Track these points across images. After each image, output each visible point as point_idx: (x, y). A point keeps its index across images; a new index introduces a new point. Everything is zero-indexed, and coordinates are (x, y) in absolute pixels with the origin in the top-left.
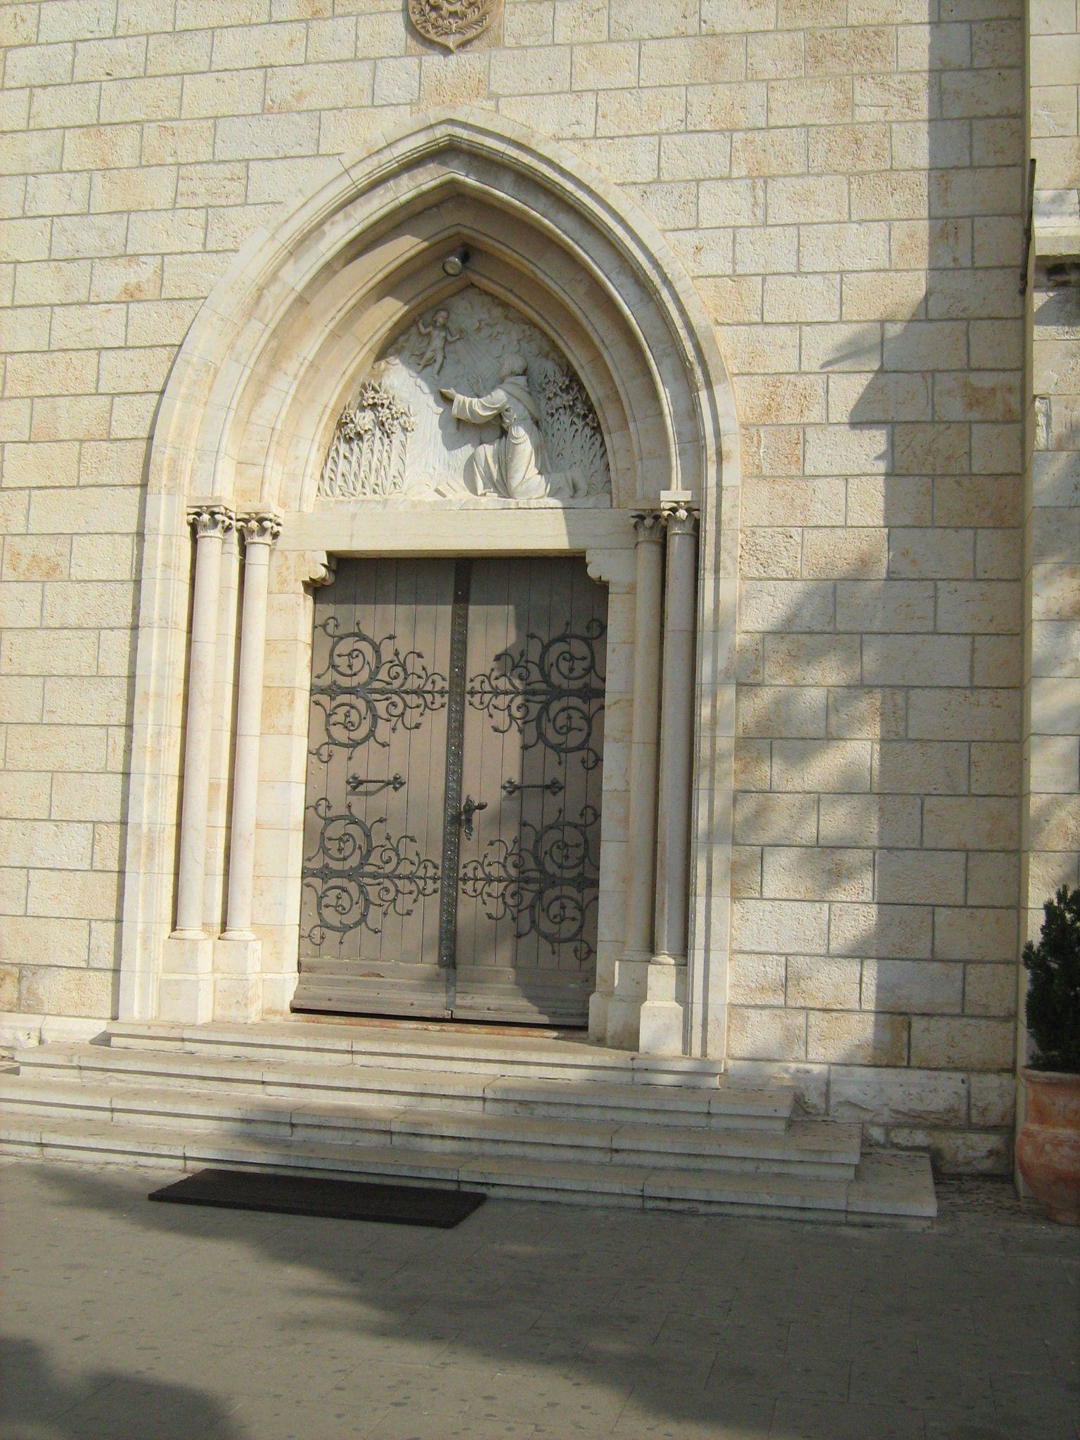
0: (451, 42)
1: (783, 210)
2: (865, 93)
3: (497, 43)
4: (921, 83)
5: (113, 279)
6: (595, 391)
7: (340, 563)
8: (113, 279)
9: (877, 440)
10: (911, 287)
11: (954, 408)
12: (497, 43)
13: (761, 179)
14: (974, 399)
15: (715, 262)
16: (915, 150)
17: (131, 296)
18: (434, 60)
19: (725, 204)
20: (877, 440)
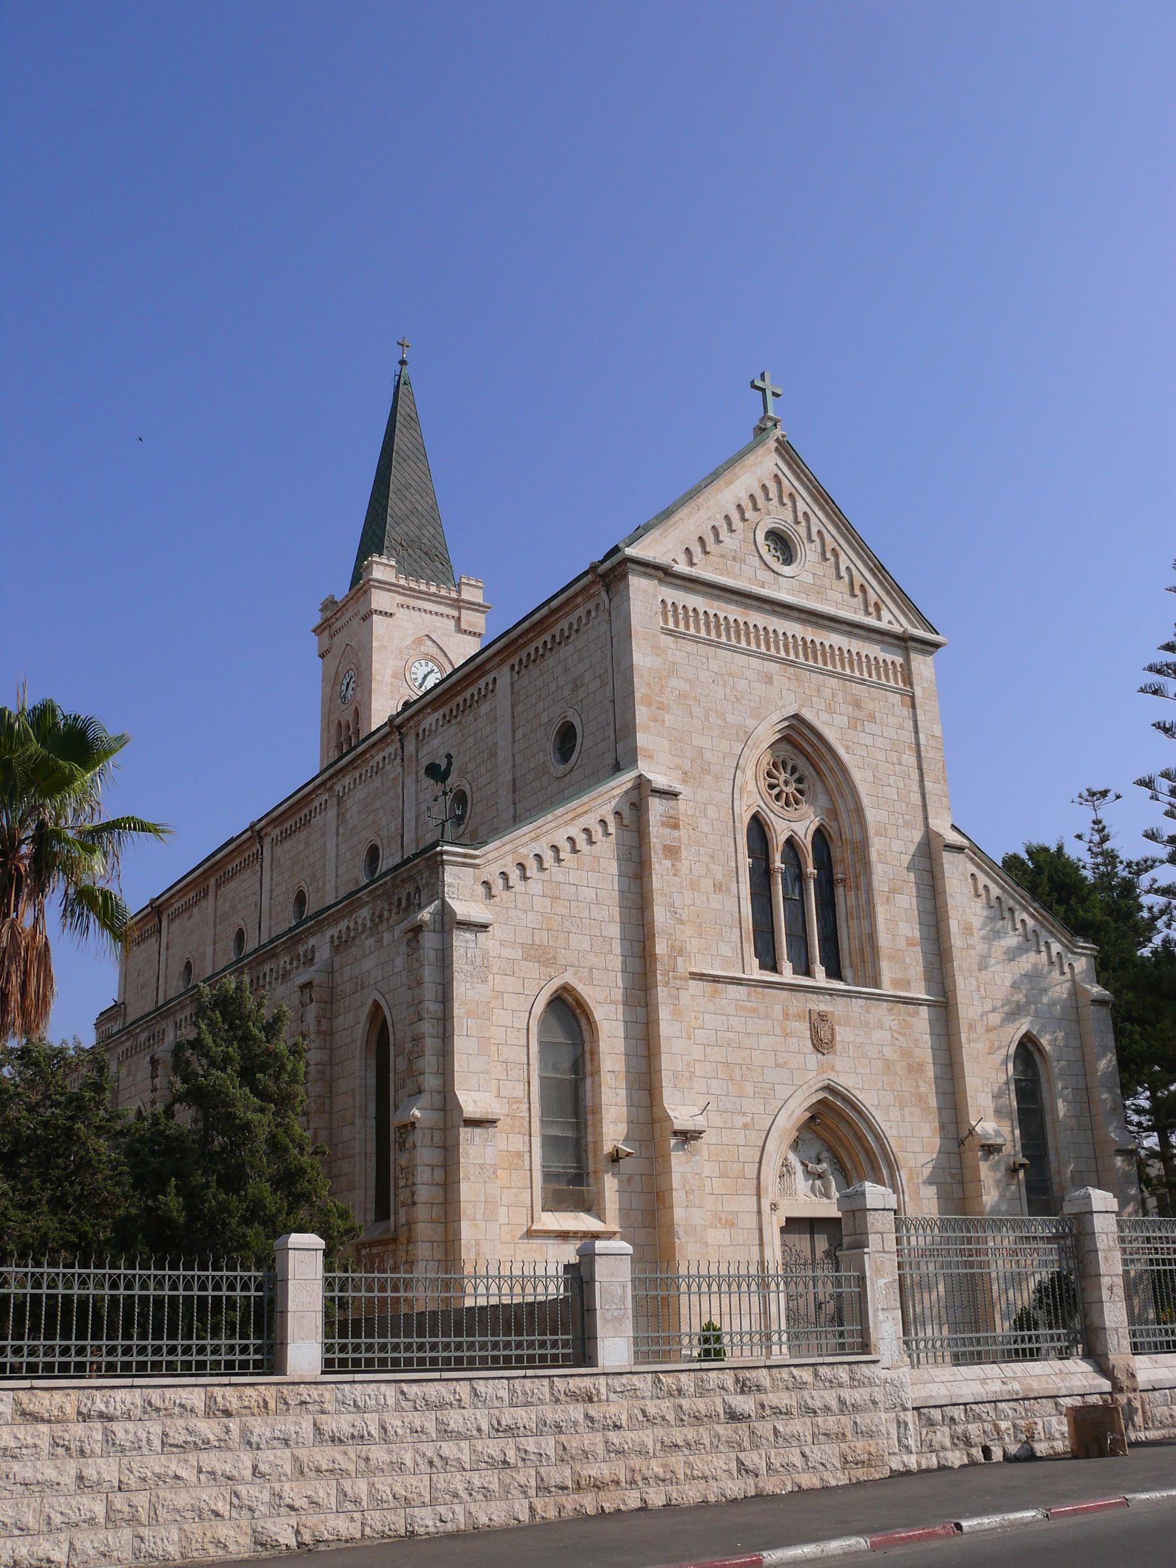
0: (825, 1051)
1: (908, 1119)
2: (921, 1084)
3: (835, 1053)
4: (932, 1081)
5: (739, 1121)
6: (849, 1165)
7: (788, 1219)
8: (739, 1121)
9: (934, 1189)
10: (937, 1142)
11: (949, 1180)
12: (835, 1053)
13: (902, 1107)
14: (953, 1176)
15: (895, 1133)
16: (933, 1102)
17: (745, 1127)
18: (820, 1056)
19: (895, 1113)
20: (934, 1189)
